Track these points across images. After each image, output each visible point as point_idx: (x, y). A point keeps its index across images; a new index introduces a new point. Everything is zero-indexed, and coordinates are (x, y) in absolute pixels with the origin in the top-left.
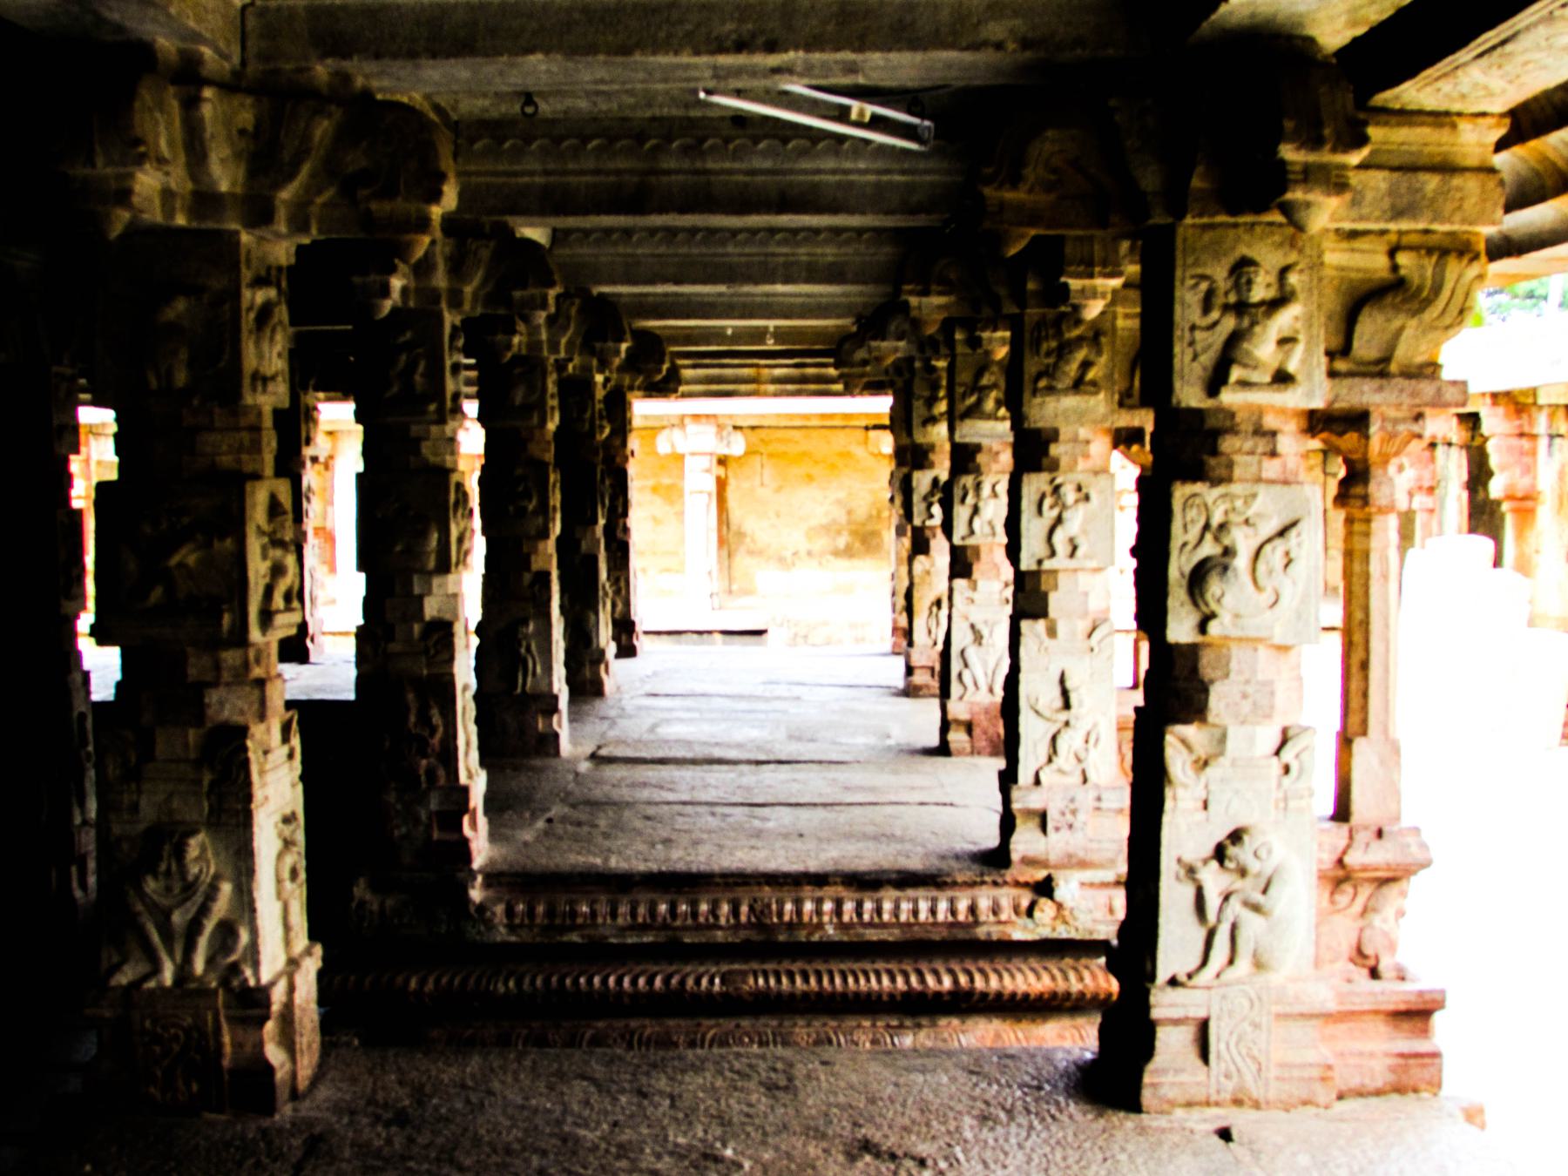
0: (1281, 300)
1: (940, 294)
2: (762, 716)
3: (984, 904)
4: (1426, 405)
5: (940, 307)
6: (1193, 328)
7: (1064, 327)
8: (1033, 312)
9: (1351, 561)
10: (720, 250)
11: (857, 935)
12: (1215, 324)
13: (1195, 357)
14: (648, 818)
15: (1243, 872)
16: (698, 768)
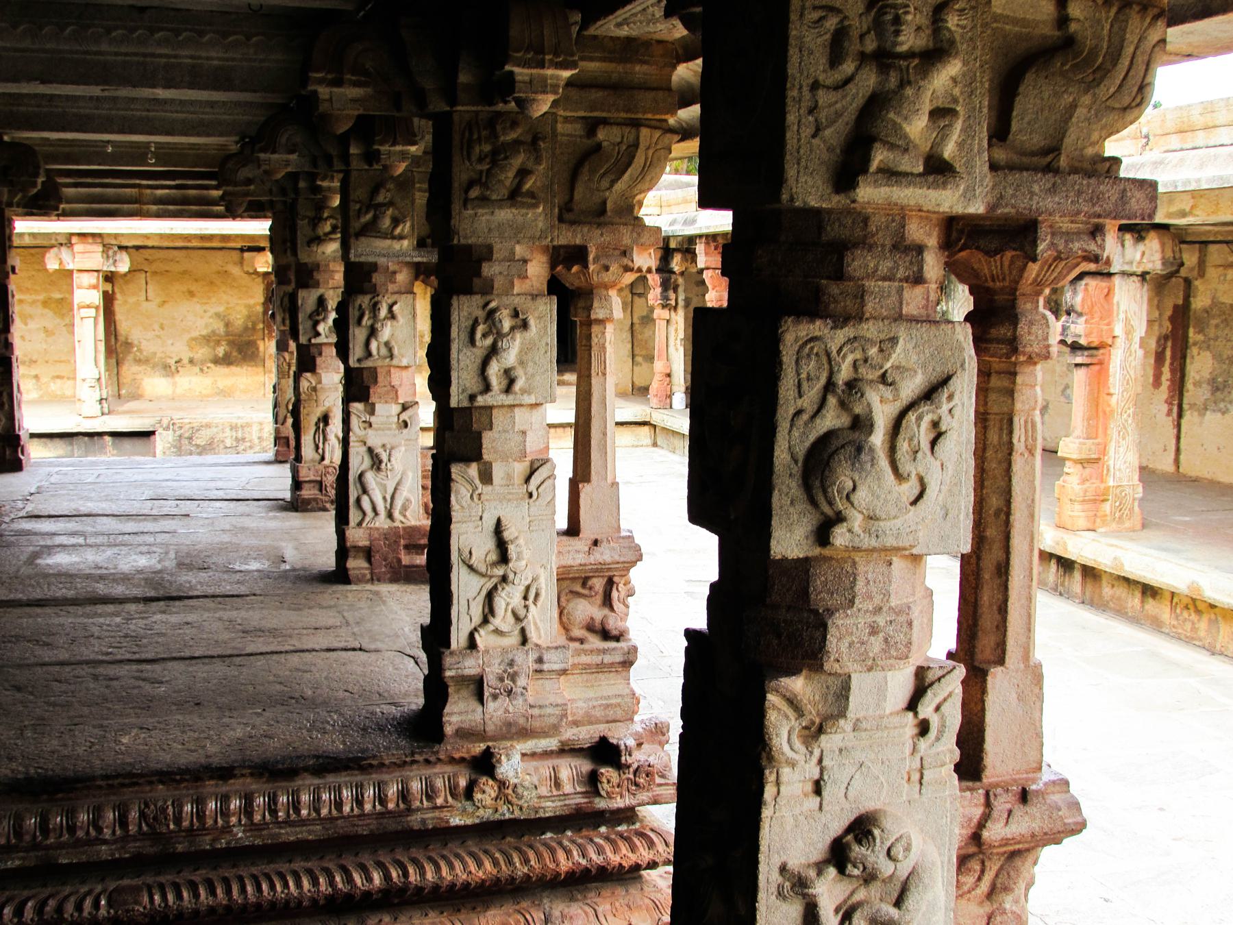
0: (934, 55)
1: (356, 84)
2: (150, 539)
3: (416, 786)
4: (1107, 216)
5: (354, 100)
6: (815, 86)
7: (499, 128)
8: (464, 109)
9: (985, 428)
10: (94, 49)
11: (272, 836)
12: (848, 81)
13: (818, 130)
14: (18, 689)
15: (869, 877)
16: (80, 610)
